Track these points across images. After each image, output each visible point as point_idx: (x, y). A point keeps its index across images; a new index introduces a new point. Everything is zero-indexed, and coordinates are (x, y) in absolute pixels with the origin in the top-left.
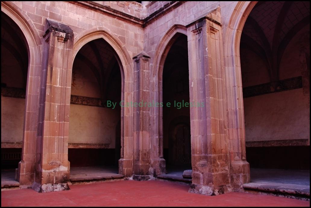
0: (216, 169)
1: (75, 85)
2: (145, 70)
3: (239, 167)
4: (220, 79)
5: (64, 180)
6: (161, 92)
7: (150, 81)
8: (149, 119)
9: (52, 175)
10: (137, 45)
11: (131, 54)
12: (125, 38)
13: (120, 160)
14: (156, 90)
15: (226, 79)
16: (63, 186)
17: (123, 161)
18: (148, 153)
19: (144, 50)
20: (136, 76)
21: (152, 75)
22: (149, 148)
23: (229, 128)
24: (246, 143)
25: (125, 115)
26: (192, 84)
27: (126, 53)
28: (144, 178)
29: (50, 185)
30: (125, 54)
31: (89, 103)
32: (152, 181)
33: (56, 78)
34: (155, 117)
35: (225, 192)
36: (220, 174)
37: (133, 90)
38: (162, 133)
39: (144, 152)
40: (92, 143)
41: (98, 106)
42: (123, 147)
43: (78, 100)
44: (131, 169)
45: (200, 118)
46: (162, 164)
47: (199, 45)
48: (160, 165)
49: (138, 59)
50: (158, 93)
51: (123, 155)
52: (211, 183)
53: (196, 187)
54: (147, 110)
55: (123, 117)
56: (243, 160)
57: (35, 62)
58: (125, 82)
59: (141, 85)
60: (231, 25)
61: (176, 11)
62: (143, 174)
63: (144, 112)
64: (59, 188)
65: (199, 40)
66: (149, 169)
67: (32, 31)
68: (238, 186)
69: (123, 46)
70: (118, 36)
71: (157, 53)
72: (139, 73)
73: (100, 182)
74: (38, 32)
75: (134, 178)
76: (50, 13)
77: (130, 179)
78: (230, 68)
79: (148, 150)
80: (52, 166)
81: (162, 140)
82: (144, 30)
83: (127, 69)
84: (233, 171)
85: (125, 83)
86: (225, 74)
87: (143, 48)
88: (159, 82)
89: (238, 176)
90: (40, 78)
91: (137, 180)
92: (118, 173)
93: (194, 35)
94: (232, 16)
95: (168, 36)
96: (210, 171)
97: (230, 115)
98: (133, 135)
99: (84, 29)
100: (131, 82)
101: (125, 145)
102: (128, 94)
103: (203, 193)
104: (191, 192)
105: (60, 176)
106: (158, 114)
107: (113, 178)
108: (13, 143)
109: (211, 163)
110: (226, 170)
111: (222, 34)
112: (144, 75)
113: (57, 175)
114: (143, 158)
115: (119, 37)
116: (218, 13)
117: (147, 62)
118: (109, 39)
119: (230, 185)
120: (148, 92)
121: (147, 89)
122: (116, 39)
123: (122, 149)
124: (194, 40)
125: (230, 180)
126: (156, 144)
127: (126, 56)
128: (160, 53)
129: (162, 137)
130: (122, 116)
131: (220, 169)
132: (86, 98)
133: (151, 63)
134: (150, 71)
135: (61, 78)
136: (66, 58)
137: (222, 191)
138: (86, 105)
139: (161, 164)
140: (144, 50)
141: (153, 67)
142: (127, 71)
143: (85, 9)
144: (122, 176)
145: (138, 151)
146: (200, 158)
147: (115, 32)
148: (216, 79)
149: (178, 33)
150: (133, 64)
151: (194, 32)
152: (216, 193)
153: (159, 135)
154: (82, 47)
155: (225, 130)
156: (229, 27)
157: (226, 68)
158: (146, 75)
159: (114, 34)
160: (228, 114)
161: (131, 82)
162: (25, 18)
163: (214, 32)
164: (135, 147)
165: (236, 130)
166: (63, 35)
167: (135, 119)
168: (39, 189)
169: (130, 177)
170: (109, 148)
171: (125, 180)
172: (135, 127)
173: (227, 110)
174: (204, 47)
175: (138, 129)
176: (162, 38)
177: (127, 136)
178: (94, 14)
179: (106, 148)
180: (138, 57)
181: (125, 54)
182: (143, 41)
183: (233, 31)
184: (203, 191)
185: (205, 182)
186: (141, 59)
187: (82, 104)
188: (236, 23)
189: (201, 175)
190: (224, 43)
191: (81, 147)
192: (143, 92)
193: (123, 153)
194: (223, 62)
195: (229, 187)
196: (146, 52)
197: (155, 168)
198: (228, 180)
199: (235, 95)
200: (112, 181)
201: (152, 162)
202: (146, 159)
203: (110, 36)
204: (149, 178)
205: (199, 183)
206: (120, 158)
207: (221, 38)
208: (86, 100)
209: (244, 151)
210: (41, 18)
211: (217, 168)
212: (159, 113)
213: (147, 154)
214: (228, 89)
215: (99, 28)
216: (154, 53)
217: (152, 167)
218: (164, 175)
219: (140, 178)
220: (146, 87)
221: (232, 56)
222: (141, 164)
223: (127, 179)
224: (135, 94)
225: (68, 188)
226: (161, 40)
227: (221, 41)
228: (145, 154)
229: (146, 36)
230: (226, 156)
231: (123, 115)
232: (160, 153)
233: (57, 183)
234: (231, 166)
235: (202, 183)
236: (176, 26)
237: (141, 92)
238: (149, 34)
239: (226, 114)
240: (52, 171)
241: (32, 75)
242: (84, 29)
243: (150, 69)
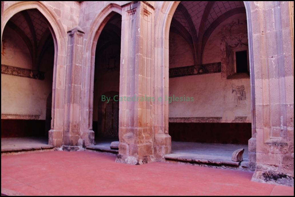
0: (141, 141)
1: (4, 54)
2: (79, 44)
3: (162, 139)
4: (150, 58)
7: (83, 56)
8: (80, 93)
10: (72, 19)
13: (50, 131)
14: (89, 64)
15: (154, 59)
17: (53, 133)
18: (78, 124)
19: (79, 25)
21: (85, 50)
22: (79, 120)
23: (154, 103)
24: (170, 118)
25: (57, 87)
26: (123, 61)
27: (61, 26)
28: (73, 148)
30: (60, 27)
31: (20, 73)
32: (81, 152)
34: (86, 91)
35: (148, 162)
36: (145, 146)
37: (65, 63)
39: (75, 124)
40: (21, 114)
41: (29, 77)
42: (54, 118)
43: (8, 71)
44: (61, 140)
45: (129, 93)
46: (91, 136)
47: (132, 25)
49: (72, 33)
50: (90, 67)
51: (53, 126)
52: (136, 154)
53: (122, 157)
54: (79, 83)
55: (55, 90)
56: (166, 134)
58: (58, 54)
59: (74, 59)
60: (163, 10)
62: (72, 145)
63: (76, 85)
65: (133, 21)
66: (78, 140)
68: (160, 157)
69: (58, 19)
70: (53, 9)
71: (91, 30)
72: (72, 47)
73: (29, 152)
75: (63, 149)
77: (59, 149)
81: (92, 113)
82: (80, 5)
84: (157, 143)
85: (58, 56)
86: (154, 54)
87: (78, 22)
88: (92, 58)
89: (161, 148)
91: (66, 150)
92: (47, 144)
93: (128, 15)
95: (104, 13)
96: (135, 143)
97: (156, 93)
98: (64, 107)
100: (64, 55)
101: (55, 116)
102: (61, 67)
103: (129, 163)
104: (118, 162)
106: (89, 88)
107: (43, 149)
109: (137, 136)
110: (150, 142)
111: (154, 17)
112: (78, 49)
114: (73, 130)
115: (55, 10)
117: (82, 37)
118: (44, 10)
119: (153, 155)
120: (81, 67)
121: (79, 64)
122: (51, 11)
123: (52, 121)
124: (127, 20)
125: (153, 151)
126: (86, 117)
127: (60, 29)
128: (94, 29)
129: (92, 110)
130: (53, 88)
131: (145, 141)
132: (17, 68)
133: (85, 38)
134: (84, 46)
137: (145, 161)
138: (17, 75)
139: (90, 136)
140: (79, 25)
141: (87, 43)
142: (61, 43)
144: (52, 146)
145: (69, 123)
146: (127, 131)
148: (146, 58)
149: (113, 12)
150: (67, 37)
151: (129, 13)
152: (141, 162)
153: (90, 108)
155: (151, 105)
156: (162, 11)
157: (156, 48)
159: (49, 5)
160: (154, 91)
161: (64, 55)
163: (147, 14)
164: (66, 119)
167: (67, 92)
169: (59, 147)
170: (39, 119)
171: (55, 150)
172: (66, 99)
173: (154, 88)
174: (137, 27)
175: (69, 101)
176: (97, 15)
177: (58, 107)
179: (36, 119)
180: (73, 31)
181: (60, 27)
182: (78, 16)
183: (165, 15)
184: (129, 161)
185: (131, 153)
187: (13, 74)
188: (168, 8)
189: (127, 146)
190: (155, 26)
191: (10, 117)
192: (76, 66)
193: (53, 124)
195: (152, 157)
196: (81, 28)
197: (84, 139)
198: (151, 151)
199: (162, 74)
200: (41, 151)
201: (82, 134)
202: (76, 131)
204: (78, 149)
205: (125, 153)
206: (50, 128)
207: (153, 20)
208: (17, 71)
209: (167, 126)
211: (142, 140)
212: (90, 87)
213: (76, 126)
214: (156, 68)
216: (89, 29)
217: (81, 138)
218: (93, 146)
219: (69, 148)
220: (79, 61)
221: (162, 38)
222: (70, 135)
223: (56, 150)
224: (68, 68)
228: (75, 126)
229: (82, 12)
230: (151, 130)
231: (55, 87)
232: (89, 125)
234: (154, 138)
235: (128, 154)
237: (74, 66)
238: (85, 10)
239: (152, 91)
243: (84, 44)
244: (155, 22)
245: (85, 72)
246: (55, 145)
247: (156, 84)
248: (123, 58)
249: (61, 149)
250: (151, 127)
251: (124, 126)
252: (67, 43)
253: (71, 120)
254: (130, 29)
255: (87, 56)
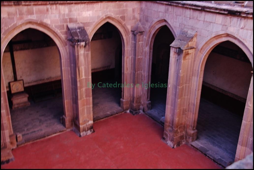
5: (91, 128)
6: (151, 58)
7: (144, 50)
8: (142, 76)
9: (85, 127)
10: (134, 18)
11: (129, 27)
12: (125, 16)
13: (121, 99)
14: (148, 57)
15: (191, 84)
16: (91, 131)
18: (140, 97)
20: (133, 45)
23: (188, 111)
26: (169, 85)
27: (126, 28)
28: (136, 113)
29: (85, 133)
33: (82, 73)
34: (146, 75)
35: (180, 145)
37: (131, 55)
38: (152, 47)
41: (101, 39)
44: (128, 106)
45: (172, 105)
48: (147, 106)
57: (64, 58)
60: (202, 51)
61: (167, 8)
64: (89, 132)
65: (177, 60)
67: (59, 38)
68: (188, 142)
69: (123, 23)
71: (150, 31)
74: (63, 37)
76: (69, 18)
78: (196, 78)
79: (139, 96)
80: (85, 122)
83: (127, 40)
84: (187, 134)
88: (150, 52)
89: (189, 138)
90: (69, 69)
91: (132, 114)
93: (175, 54)
94: (203, 46)
96: (173, 136)
99: (94, 22)
102: (127, 58)
104: (163, 141)
105: (89, 126)
106: (148, 74)
108: (44, 80)
109: (174, 132)
111: (195, 54)
112: (139, 46)
113: (87, 126)
116: (195, 39)
117: (142, 36)
119: (184, 140)
120: (142, 58)
121: (141, 56)
124: (174, 58)
125: (185, 137)
127: (126, 30)
130: (123, 72)
134: (144, 42)
135: (85, 72)
136: (87, 59)
137: (179, 144)
143: (93, 4)
146: (169, 126)
147: (117, 14)
150: (131, 35)
154: (94, 34)
155: (186, 113)
156: (200, 52)
157: (193, 77)
158: (140, 46)
162: (54, 30)
164: (132, 93)
165: (192, 114)
166: (83, 44)
167: (132, 75)
168: (79, 135)
173: (189, 102)
178: (101, 5)
180: (135, 32)
183: (202, 55)
186: (137, 35)
188: (205, 50)
190: (194, 61)
194: (192, 73)
198: (184, 138)
201: (142, 103)
203: (113, 19)
204: (140, 112)
206: (121, 97)
207: (193, 57)
210: (64, 25)
213: (139, 98)
215: (106, 16)
217: (142, 105)
224: (132, 59)
225: (94, 131)
226: (154, 23)
227: (193, 60)
228: (138, 98)
230: (184, 127)
232: (148, 98)
233: (88, 130)
236: (165, 21)
237: (137, 58)
240: (85, 125)
241: (64, 67)
242: (94, 22)
244: (195, 58)
245: (145, 62)
246: (125, 109)
247: (191, 100)
248: (169, 84)
249: (128, 111)
250: (185, 125)
251: (167, 123)
252: (131, 40)
253: (135, 96)
254: (175, 65)
255: (147, 50)
